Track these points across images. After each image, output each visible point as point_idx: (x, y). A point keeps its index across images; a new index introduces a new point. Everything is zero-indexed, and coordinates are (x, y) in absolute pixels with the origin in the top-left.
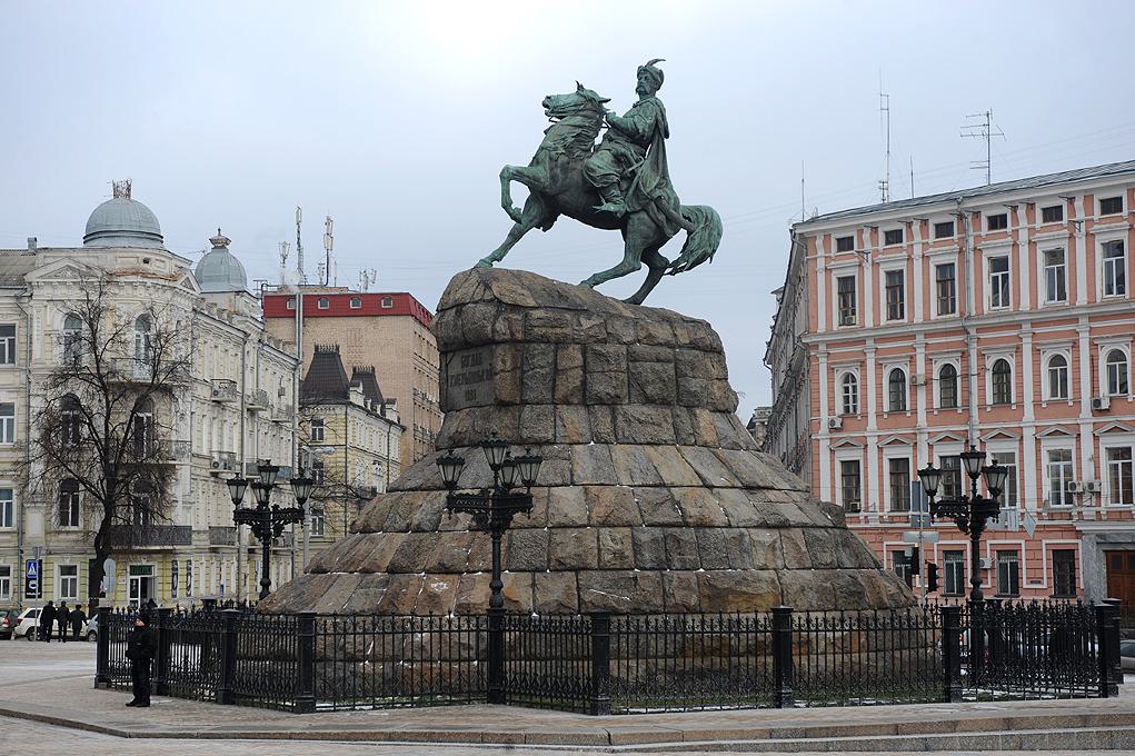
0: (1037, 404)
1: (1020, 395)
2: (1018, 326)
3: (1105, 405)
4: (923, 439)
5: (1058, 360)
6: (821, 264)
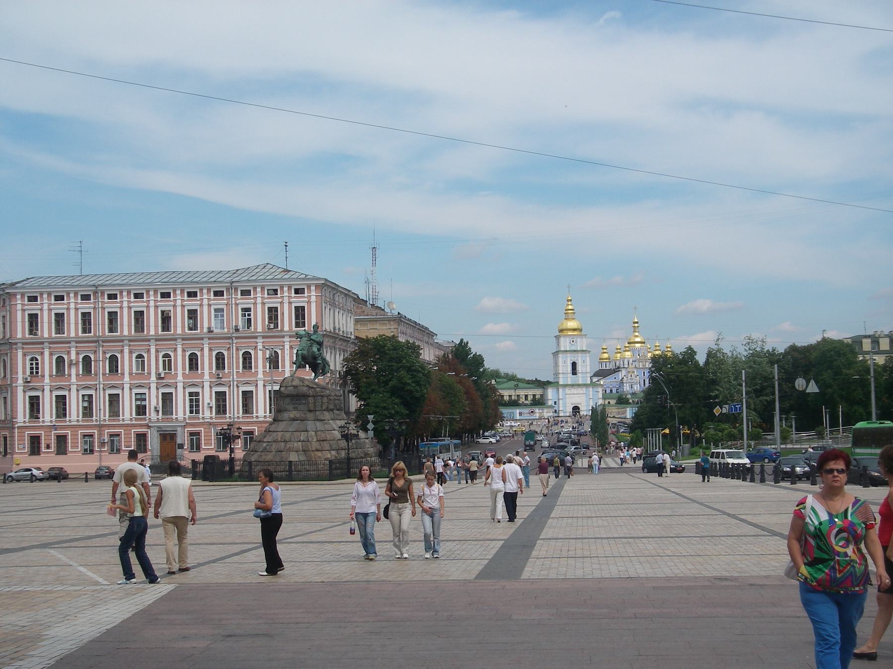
0: (131, 374)
1: (123, 369)
2: (122, 341)
3: (162, 376)
4: (74, 388)
5: (140, 356)
6: (19, 307)
